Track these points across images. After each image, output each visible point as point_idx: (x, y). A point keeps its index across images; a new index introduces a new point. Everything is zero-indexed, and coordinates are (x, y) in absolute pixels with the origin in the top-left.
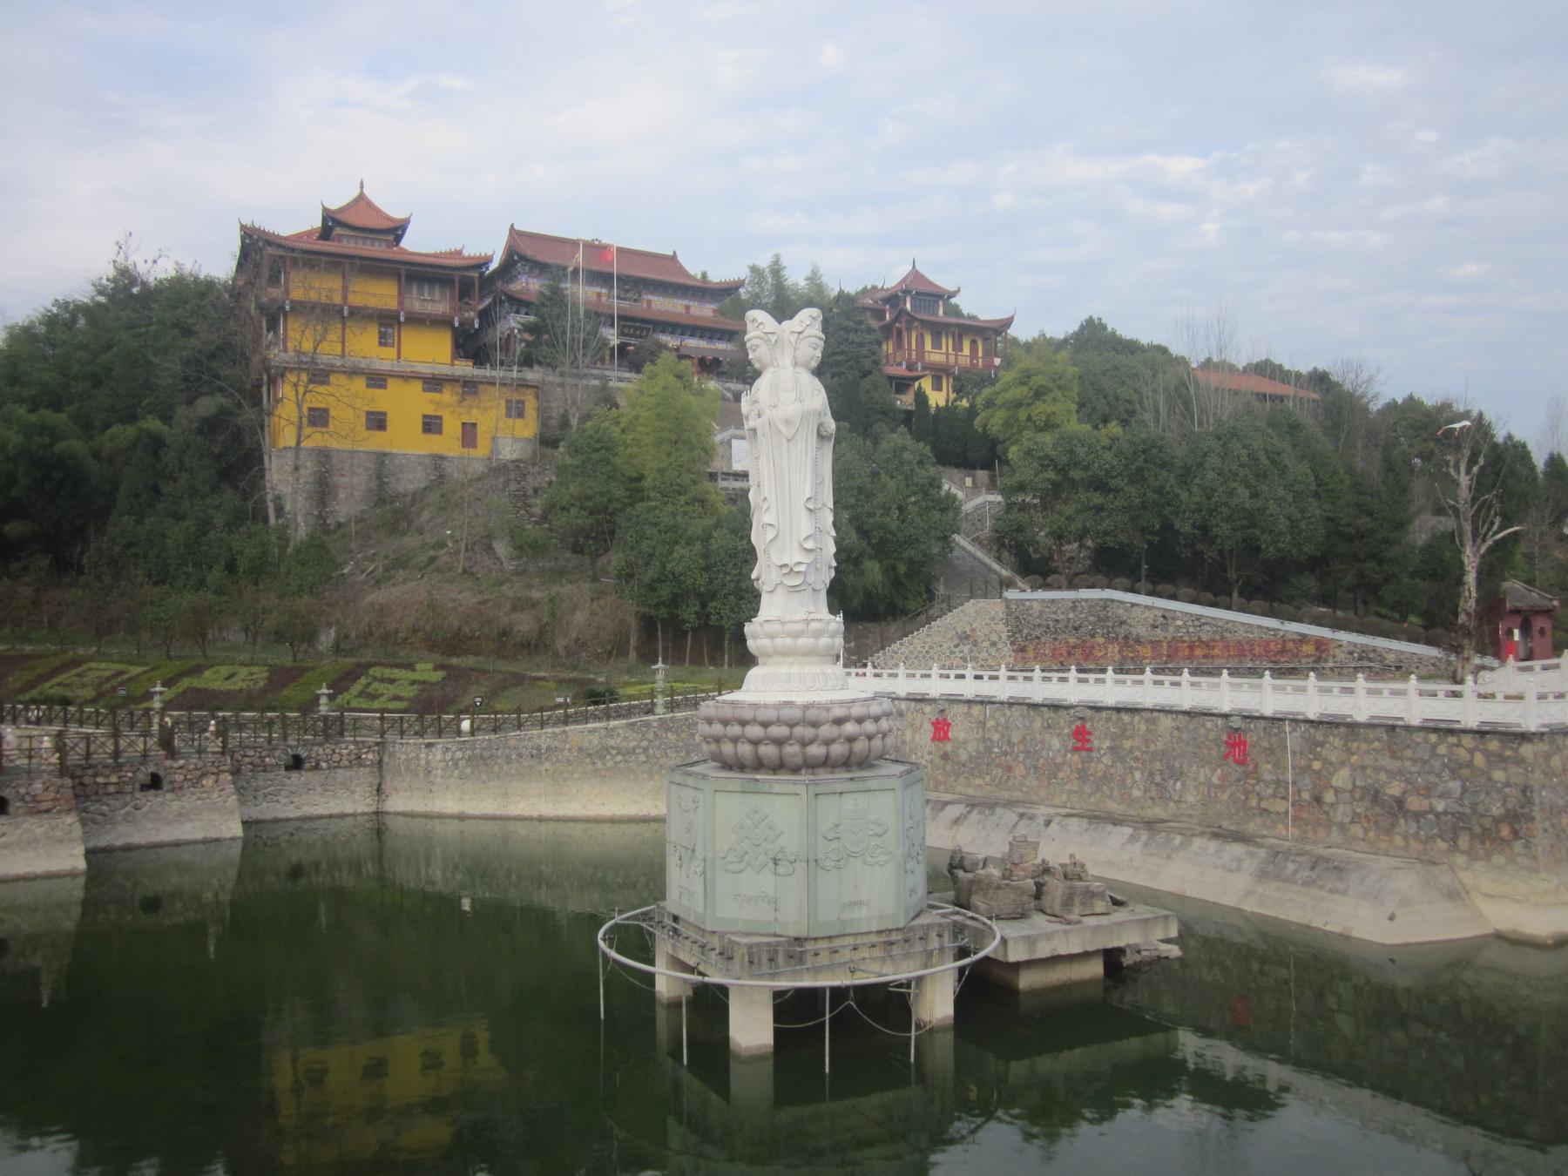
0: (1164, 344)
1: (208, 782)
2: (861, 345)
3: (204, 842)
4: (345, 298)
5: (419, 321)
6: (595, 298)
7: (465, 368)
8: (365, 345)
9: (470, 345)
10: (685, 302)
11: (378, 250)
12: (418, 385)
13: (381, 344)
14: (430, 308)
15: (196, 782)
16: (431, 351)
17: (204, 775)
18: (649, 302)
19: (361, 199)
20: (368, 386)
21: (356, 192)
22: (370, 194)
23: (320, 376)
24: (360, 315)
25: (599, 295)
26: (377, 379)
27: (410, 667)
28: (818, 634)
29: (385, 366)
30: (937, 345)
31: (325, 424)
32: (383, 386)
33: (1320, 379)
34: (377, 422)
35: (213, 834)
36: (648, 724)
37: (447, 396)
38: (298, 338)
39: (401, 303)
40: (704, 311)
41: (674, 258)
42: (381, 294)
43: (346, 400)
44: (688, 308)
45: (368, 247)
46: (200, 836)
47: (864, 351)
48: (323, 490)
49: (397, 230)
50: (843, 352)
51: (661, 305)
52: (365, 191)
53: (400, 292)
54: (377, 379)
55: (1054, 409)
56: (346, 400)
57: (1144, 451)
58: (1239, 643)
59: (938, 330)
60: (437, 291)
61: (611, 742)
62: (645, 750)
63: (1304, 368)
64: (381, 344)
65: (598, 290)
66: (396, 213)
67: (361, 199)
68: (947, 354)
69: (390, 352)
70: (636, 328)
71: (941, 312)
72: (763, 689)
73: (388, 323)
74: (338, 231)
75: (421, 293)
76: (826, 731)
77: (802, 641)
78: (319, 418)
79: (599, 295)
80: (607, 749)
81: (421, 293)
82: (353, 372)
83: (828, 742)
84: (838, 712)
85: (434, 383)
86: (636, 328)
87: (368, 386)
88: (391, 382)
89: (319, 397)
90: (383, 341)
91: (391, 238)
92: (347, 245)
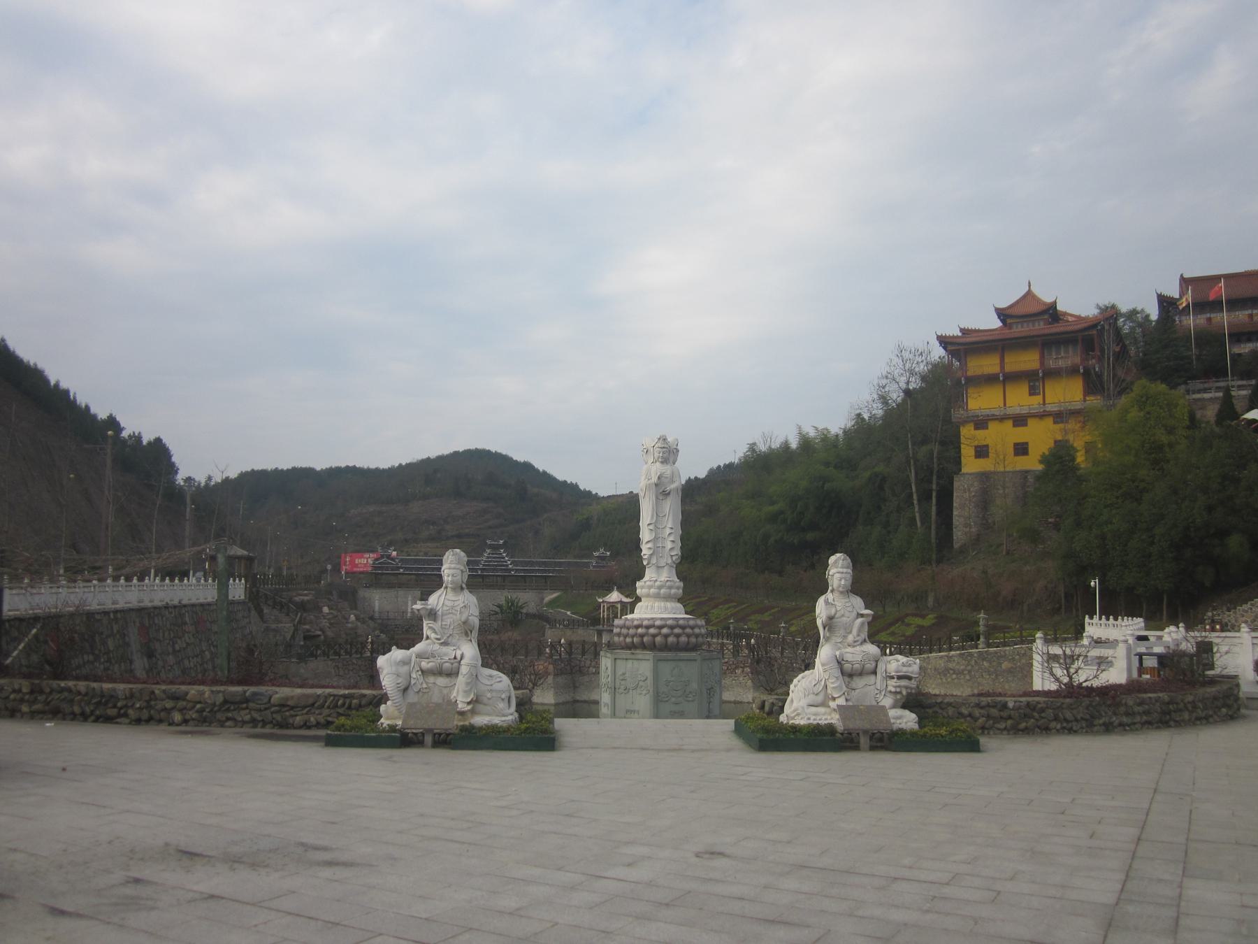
1: (739, 671)
3: (735, 702)
4: (1002, 367)
5: (1052, 374)
6: (1247, 319)
7: (1095, 401)
8: (1020, 399)
9: (1093, 385)
11: (1040, 327)
12: (1050, 421)
13: (1031, 394)
14: (1061, 363)
15: (733, 671)
16: (1067, 393)
17: (737, 667)
20: (1015, 426)
22: (1037, 291)
23: (981, 423)
24: (1011, 378)
26: (1020, 421)
27: (923, 617)
28: (670, 588)
29: (1025, 411)
32: (1026, 425)
34: (1021, 449)
35: (738, 699)
36: (971, 655)
37: (1072, 425)
39: (1042, 363)
42: (1028, 360)
43: (1000, 436)
45: (1037, 327)
46: (733, 699)
48: (984, 502)
49: (1051, 313)
53: (1042, 357)
54: (1020, 421)
56: (1000, 436)
61: (950, 665)
62: (970, 672)
64: (1031, 394)
66: (1047, 298)
69: (1039, 399)
72: (642, 612)
73: (1034, 380)
74: (1009, 321)
76: (632, 631)
77: (652, 590)
78: (982, 452)
79: (1251, 316)
80: (947, 670)
82: (1002, 419)
83: (633, 637)
84: (636, 623)
85: (1059, 417)
87: (1015, 426)
88: (1031, 422)
89: (982, 436)
92: (1019, 330)
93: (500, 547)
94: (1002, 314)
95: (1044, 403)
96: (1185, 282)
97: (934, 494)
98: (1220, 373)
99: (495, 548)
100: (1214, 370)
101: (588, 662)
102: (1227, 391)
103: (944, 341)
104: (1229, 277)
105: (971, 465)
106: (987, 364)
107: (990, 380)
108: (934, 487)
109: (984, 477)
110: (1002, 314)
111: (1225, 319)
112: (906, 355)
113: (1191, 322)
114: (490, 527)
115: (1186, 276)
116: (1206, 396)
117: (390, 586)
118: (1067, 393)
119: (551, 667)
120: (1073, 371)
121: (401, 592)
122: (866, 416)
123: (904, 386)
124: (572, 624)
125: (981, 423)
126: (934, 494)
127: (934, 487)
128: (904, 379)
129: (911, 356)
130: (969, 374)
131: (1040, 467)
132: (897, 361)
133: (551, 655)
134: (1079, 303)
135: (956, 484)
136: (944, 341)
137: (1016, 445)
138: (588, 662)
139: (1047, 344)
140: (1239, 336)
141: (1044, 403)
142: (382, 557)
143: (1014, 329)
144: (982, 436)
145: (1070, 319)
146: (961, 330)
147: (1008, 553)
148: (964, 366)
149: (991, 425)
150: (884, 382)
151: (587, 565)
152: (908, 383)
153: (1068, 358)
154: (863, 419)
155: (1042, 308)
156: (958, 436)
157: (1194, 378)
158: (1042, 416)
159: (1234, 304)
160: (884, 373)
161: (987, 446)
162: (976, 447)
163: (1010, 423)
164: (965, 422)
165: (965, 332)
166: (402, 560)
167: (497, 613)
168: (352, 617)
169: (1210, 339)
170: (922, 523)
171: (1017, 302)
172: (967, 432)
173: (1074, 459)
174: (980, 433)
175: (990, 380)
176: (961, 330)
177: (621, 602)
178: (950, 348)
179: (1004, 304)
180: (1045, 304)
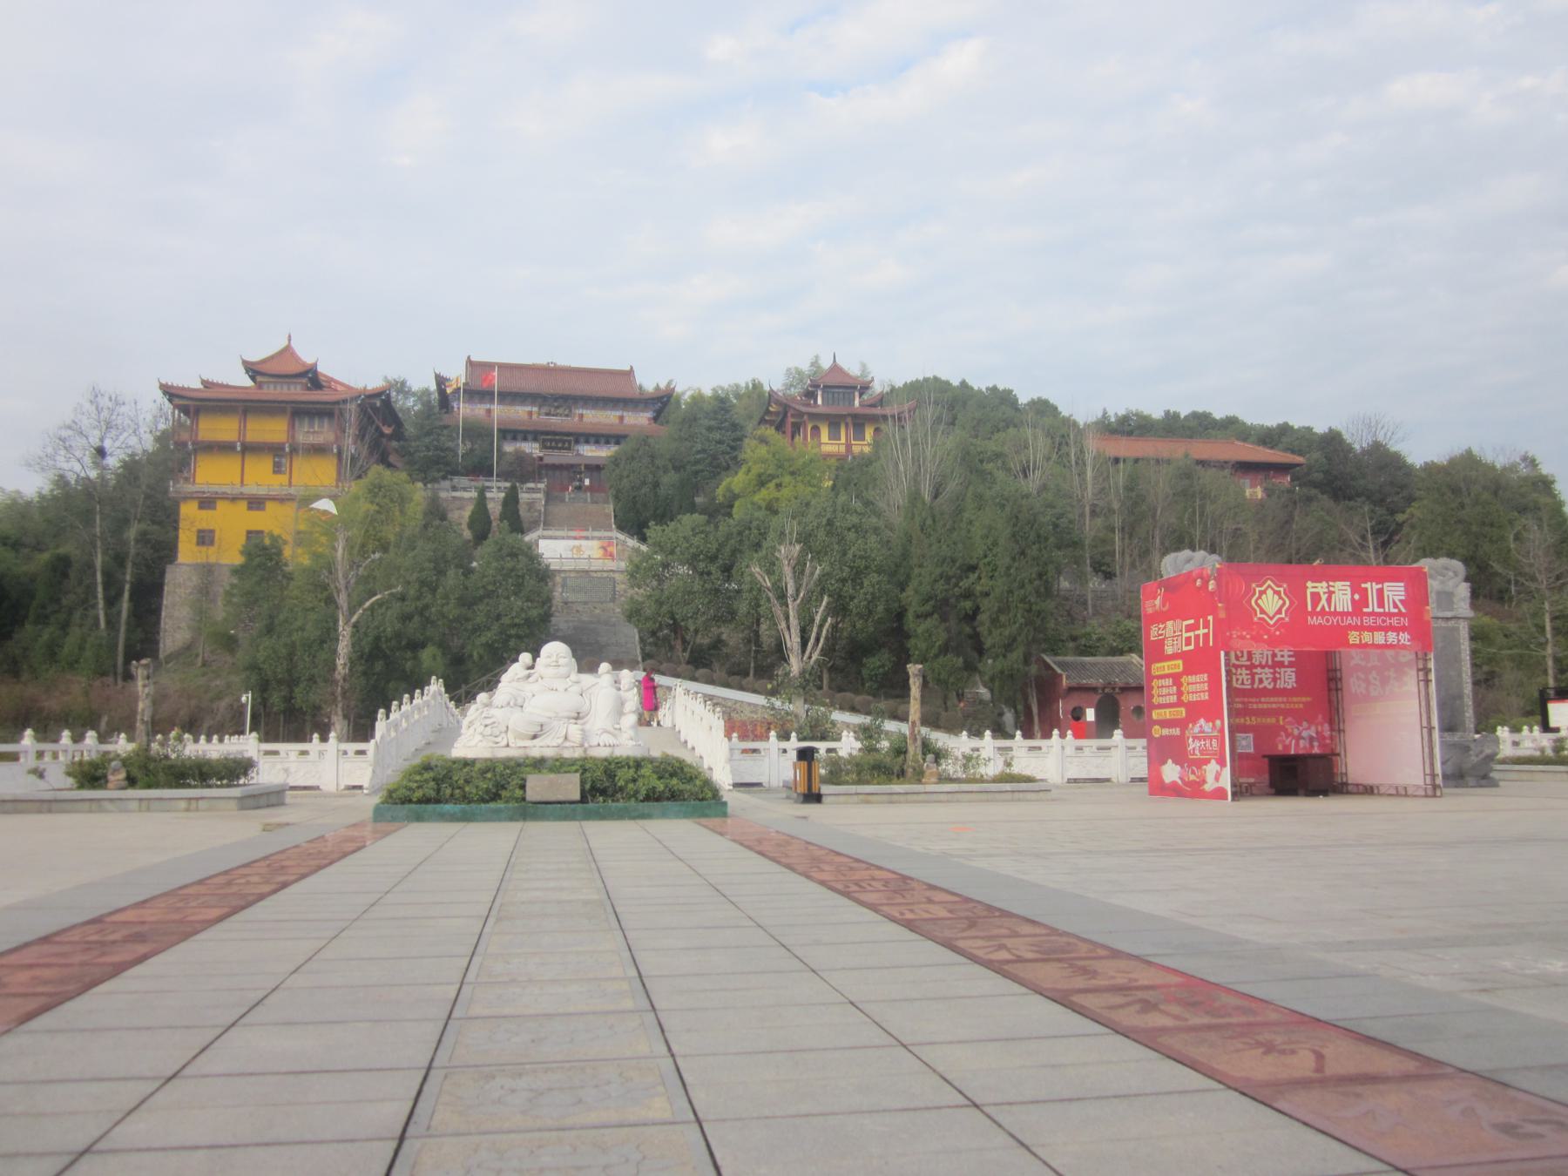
0: (1230, 413)
2: (720, 442)
6: (526, 417)
8: (260, 476)
10: (618, 413)
11: (296, 392)
16: (317, 474)
18: (581, 416)
19: (287, 352)
20: (250, 508)
21: (284, 343)
23: (207, 502)
24: (250, 449)
25: (530, 413)
29: (262, 492)
30: (834, 436)
31: (212, 543)
33: (1332, 440)
38: (211, 474)
40: (640, 419)
41: (629, 374)
42: (273, 430)
44: (621, 418)
47: (723, 447)
49: (312, 378)
50: (704, 451)
51: (594, 418)
52: (293, 344)
53: (292, 426)
54: (256, 503)
55: (777, 495)
57: (740, 533)
58: (744, 724)
59: (834, 422)
60: (326, 421)
63: (1320, 428)
65: (528, 408)
67: (287, 352)
68: (849, 446)
69: (283, 479)
70: (557, 442)
71: (857, 403)
74: (259, 379)
75: (311, 425)
78: (205, 538)
79: (530, 413)
81: (311, 425)
82: (234, 499)
86: (557, 442)
87: (250, 508)
88: (270, 505)
89: (205, 519)
90: (277, 469)
91: (304, 380)
92: (273, 392)
94: (253, 370)
95: (290, 484)
96: (471, 364)
97: (127, 587)
98: (488, 473)
100: (480, 468)
102: (482, 492)
103: (170, 393)
104: (502, 367)
105: (188, 552)
106: (223, 429)
107: (225, 448)
108: (128, 578)
109: (207, 570)
110: (253, 370)
111: (499, 412)
112: (104, 402)
113: (464, 410)
115: (474, 359)
116: (466, 495)
118: (317, 474)
120: (318, 450)
122: (72, 478)
123: (95, 442)
125: (207, 502)
126: (127, 587)
127: (128, 578)
128: (97, 433)
129: (110, 405)
130: (200, 438)
131: (238, 560)
132: (87, 406)
134: (355, 367)
135: (168, 577)
136: (170, 393)
137: (249, 532)
139: (299, 412)
140: (511, 433)
141: (290, 484)
143: (265, 390)
144: (205, 519)
145: (339, 388)
146: (204, 382)
147: (204, 665)
148: (193, 430)
149: (220, 505)
150: (65, 433)
152: (102, 440)
153: (321, 433)
154: (67, 483)
155: (301, 369)
156: (177, 512)
157: (456, 473)
158: (281, 500)
159: (509, 397)
160: (68, 422)
161: (212, 531)
162: (199, 531)
163: (243, 505)
164: (186, 499)
165: (207, 384)
169: (477, 432)
170: (108, 622)
171: (272, 357)
172: (188, 510)
173: (280, 553)
174: (204, 513)
175: (225, 448)
176: (204, 382)
178: (177, 401)
179: (255, 356)
180: (304, 364)
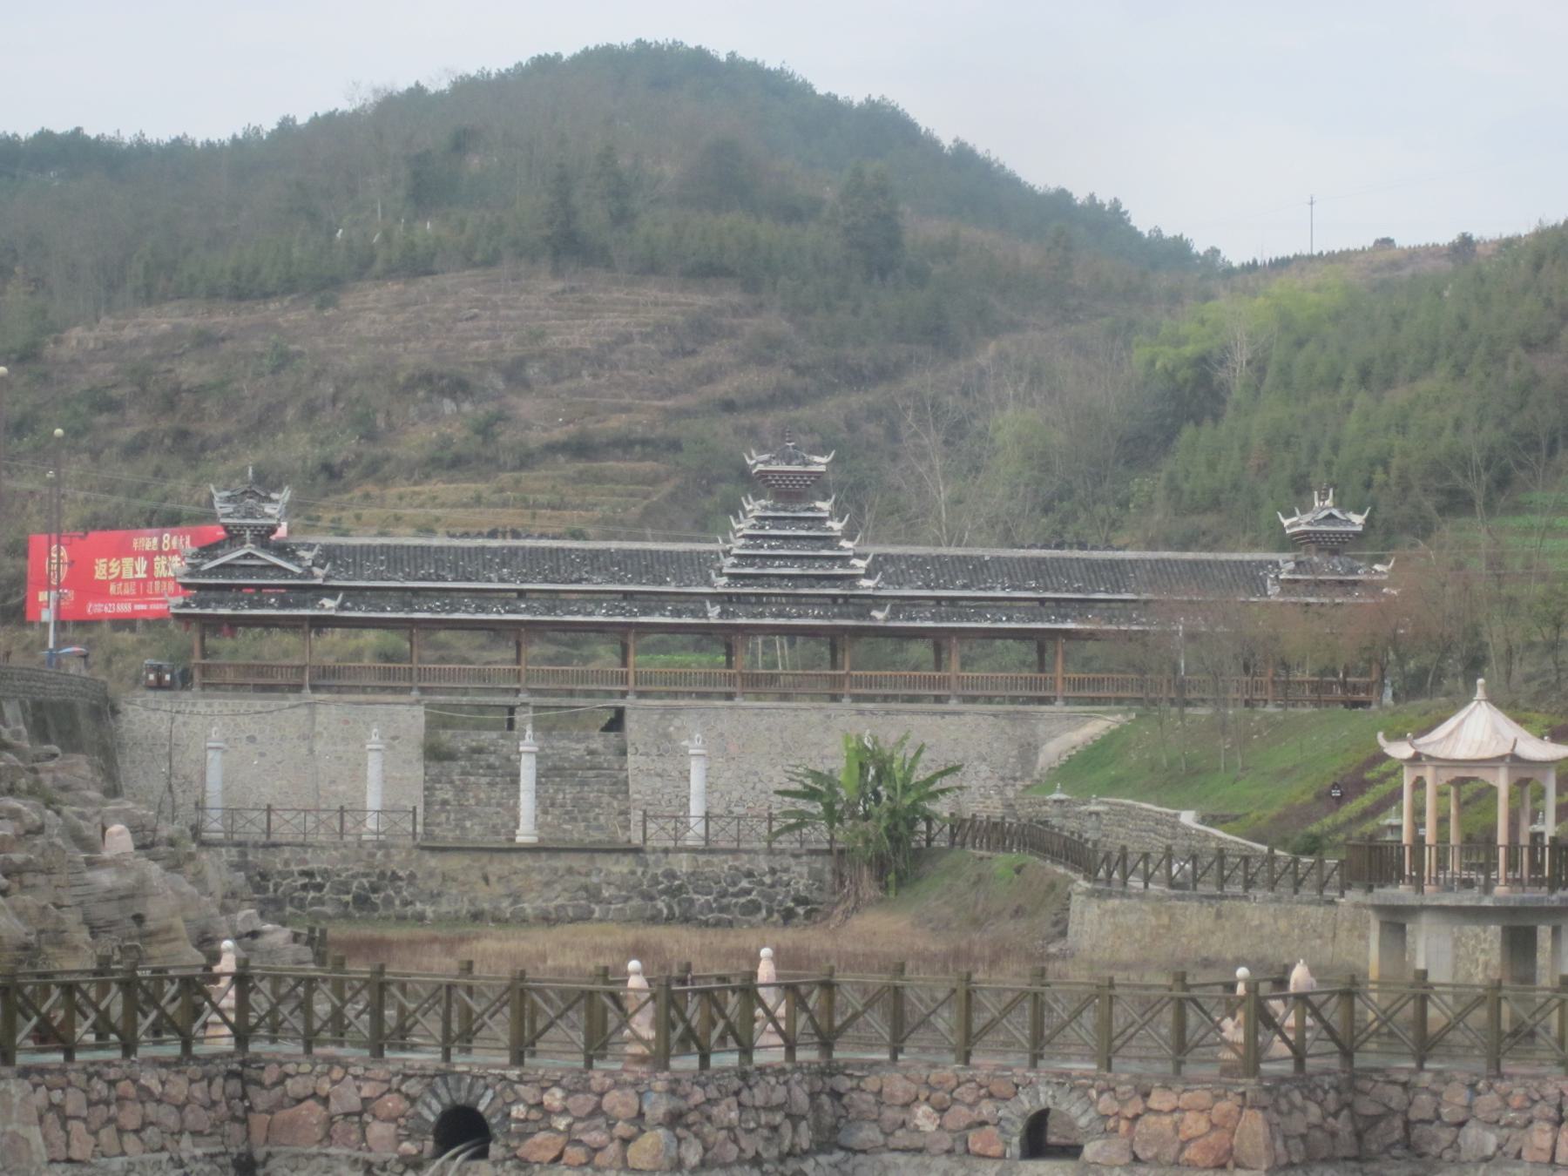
93: (817, 485)
99: (791, 491)
101: (1459, 1096)
114: (729, 406)
117: (265, 681)
119: (1254, 1125)
121: (331, 711)
124: (1213, 875)
133: (1254, 1055)
138: (1455, 1098)
142: (234, 537)
151: (1251, 577)
166: (329, 555)
167: (803, 819)
168: (119, 839)
177: (1514, 760)
